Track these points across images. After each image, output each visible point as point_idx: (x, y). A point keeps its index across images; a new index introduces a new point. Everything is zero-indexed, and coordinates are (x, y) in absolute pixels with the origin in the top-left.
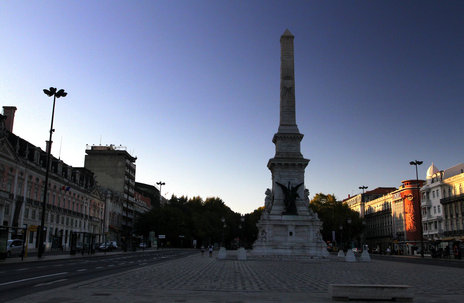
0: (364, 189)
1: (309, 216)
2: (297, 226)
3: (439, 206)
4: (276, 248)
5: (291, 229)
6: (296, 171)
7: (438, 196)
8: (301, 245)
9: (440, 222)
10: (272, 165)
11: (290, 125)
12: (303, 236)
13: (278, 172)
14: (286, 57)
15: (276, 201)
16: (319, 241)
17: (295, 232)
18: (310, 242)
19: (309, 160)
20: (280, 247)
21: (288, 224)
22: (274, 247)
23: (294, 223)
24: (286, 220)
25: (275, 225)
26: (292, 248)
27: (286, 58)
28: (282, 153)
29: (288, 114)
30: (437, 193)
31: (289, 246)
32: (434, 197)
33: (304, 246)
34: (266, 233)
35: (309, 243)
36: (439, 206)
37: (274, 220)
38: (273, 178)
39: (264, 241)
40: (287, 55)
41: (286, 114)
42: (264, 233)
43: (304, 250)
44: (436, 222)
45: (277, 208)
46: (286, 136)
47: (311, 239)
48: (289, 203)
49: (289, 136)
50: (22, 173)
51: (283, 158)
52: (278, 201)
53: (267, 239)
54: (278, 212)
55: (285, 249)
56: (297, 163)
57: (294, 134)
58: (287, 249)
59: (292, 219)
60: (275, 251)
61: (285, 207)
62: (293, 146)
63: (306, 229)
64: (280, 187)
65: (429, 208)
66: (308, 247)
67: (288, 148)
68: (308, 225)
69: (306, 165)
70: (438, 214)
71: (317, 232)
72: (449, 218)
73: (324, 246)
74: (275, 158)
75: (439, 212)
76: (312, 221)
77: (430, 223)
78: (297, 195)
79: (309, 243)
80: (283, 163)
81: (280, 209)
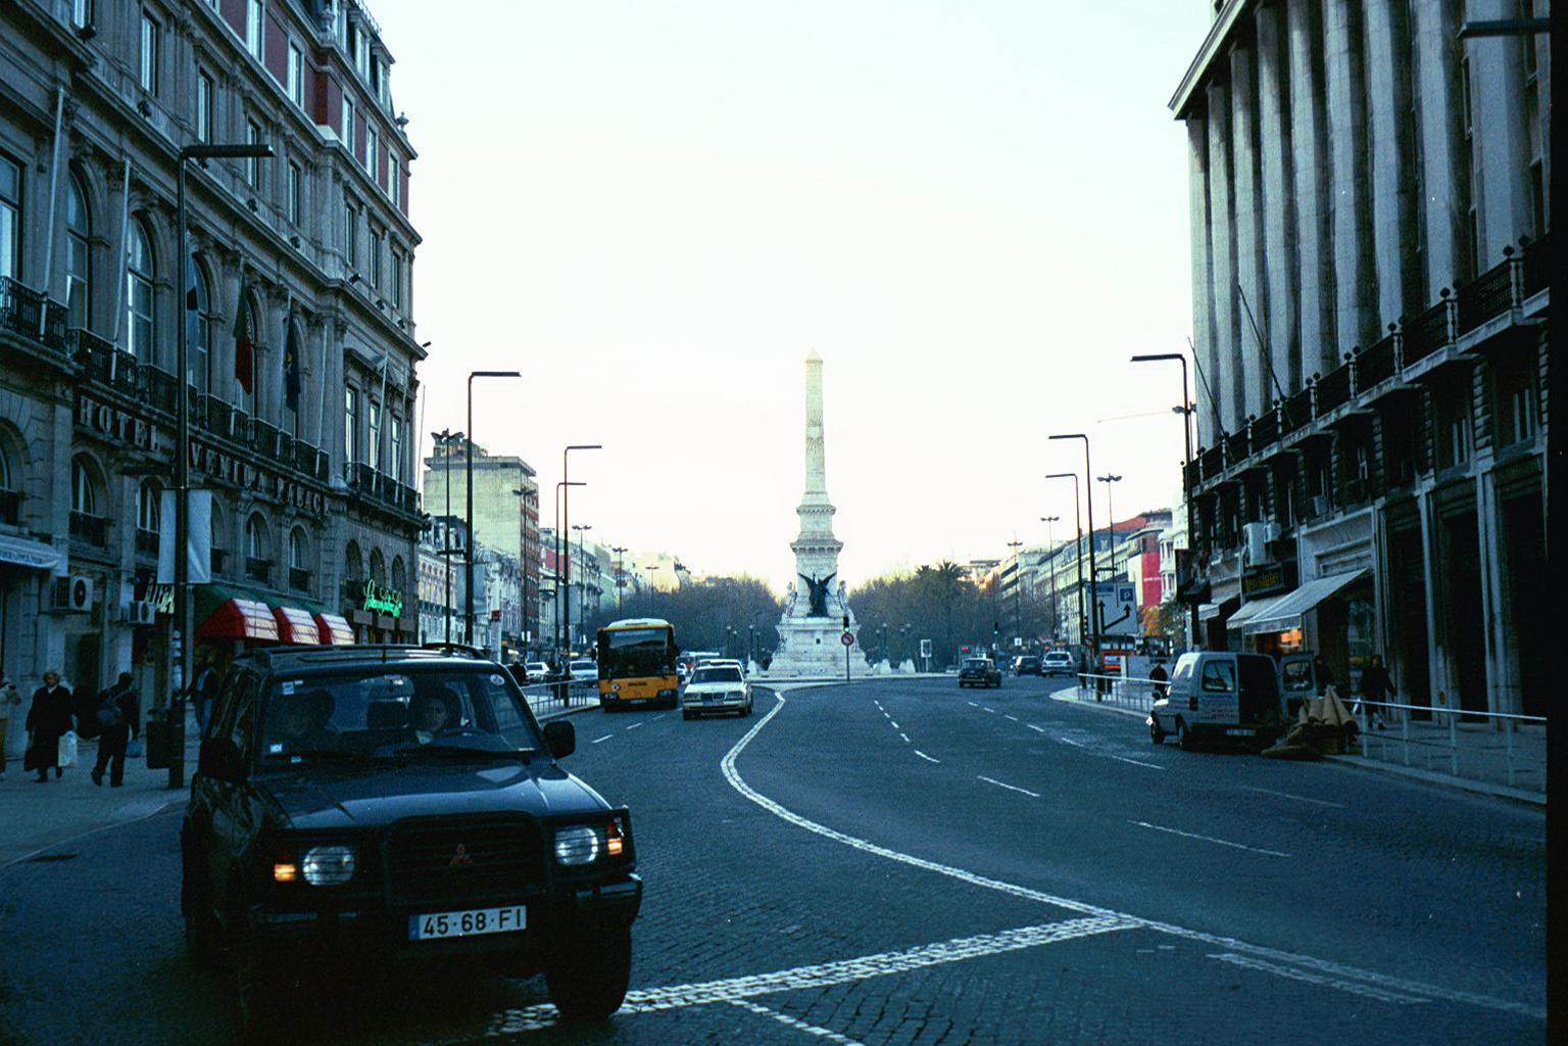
2: (826, 632)
23: (822, 628)
25: (796, 632)
26: (819, 659)
54: (801, 614)
64: (804, 581)
69: (839, 549)
78: (825, 591)
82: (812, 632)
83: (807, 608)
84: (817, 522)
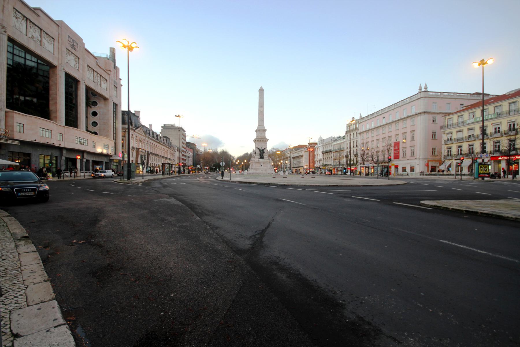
2: (264, 163)
3: (321, 154)
7: (321, 150)
9: (321, 161)
10: (255, 141)
19: (268, 139)
23: (263, 162)
25: (256, 163)
26: (262, 171)
30: (321, 149)
32: (320, 150)
36: (321, 154)
38: (255, 145)
44: (319, 161)
45: (257, 156)
46: (260, 130)
47: (269, 168)
49: (261, 130)
50: (147, 141)
51: (259, 138)
54: (257, 158)
57: (264, 129)
60: (256, 172)
63: (267, 164)
64: (258, 149)
65: (317, 155)
70: (320, 158)
72: (324, 159)
74: (256, 138)
75: (321, 156)
77: (317, 161)
78: (264, 152)
80: (259, 140)
83: (259, 157)
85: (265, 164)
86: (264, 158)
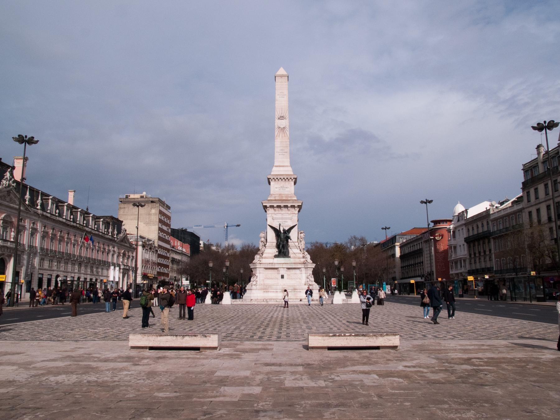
0: (387, 229)
1: (301, 258)
2: (289, 269)
4: (267, 292)
5: (282, 272)
6: (289, 212)
8: (292, 288)
11: (283, 166)
12: (294, 279)
13: (270, 214)
14: (280, 96)
15: (269, 244)
16: (311, 283)
17: (287, 275)
18: (302, 284)
20: (272, 291)
21: (280, 267)
22: (265, 291)
24: (277, 263)
25: (266, 268)
27: (280, 97)
28: (275, 194)
29: (282, 154)
31: (280, 289)
33: (295, 289)
34: (257, 277)
35: (301, 285)
37: (265, 263)
39: (255, 285)
40: (281, 94)
41: (280, 155)
42: (255, 277)
43: (295, 293)
48: (281, 246)
51: (275, 200)
52: (271, 244)
53: (258, 283)
55: (276, 292)
56: (289, 205)
57: (287, 175)
58: (277, 292)
59: (283, 262)
61: (277, 250)
62: (287, 188)
63: (297, 271)
66: (300, 289)
67: (281, 190)
68: (300, 267)
71: (309, 274)
73: (315, 288)
76: (304, 263)
78: (288, 238)
79: (301, 285)
80: (275, 205)
81: (272, 252)
82: (277, 268)
83: (275, 251)
84: (282, 187)
85: (293, 271)
86: (291, 254)
